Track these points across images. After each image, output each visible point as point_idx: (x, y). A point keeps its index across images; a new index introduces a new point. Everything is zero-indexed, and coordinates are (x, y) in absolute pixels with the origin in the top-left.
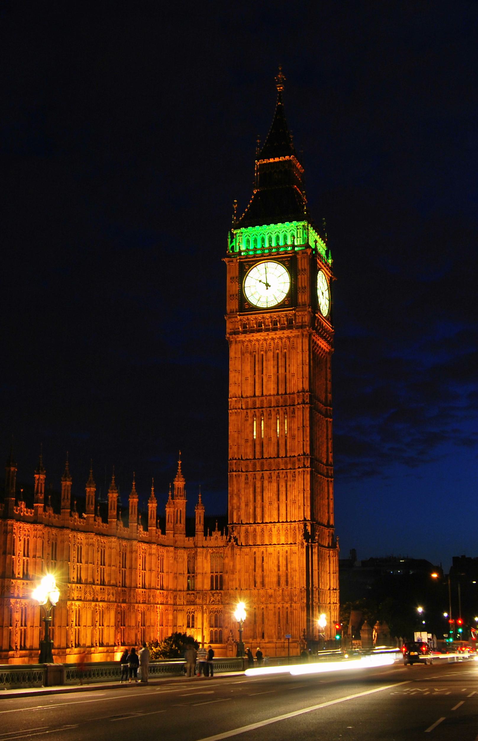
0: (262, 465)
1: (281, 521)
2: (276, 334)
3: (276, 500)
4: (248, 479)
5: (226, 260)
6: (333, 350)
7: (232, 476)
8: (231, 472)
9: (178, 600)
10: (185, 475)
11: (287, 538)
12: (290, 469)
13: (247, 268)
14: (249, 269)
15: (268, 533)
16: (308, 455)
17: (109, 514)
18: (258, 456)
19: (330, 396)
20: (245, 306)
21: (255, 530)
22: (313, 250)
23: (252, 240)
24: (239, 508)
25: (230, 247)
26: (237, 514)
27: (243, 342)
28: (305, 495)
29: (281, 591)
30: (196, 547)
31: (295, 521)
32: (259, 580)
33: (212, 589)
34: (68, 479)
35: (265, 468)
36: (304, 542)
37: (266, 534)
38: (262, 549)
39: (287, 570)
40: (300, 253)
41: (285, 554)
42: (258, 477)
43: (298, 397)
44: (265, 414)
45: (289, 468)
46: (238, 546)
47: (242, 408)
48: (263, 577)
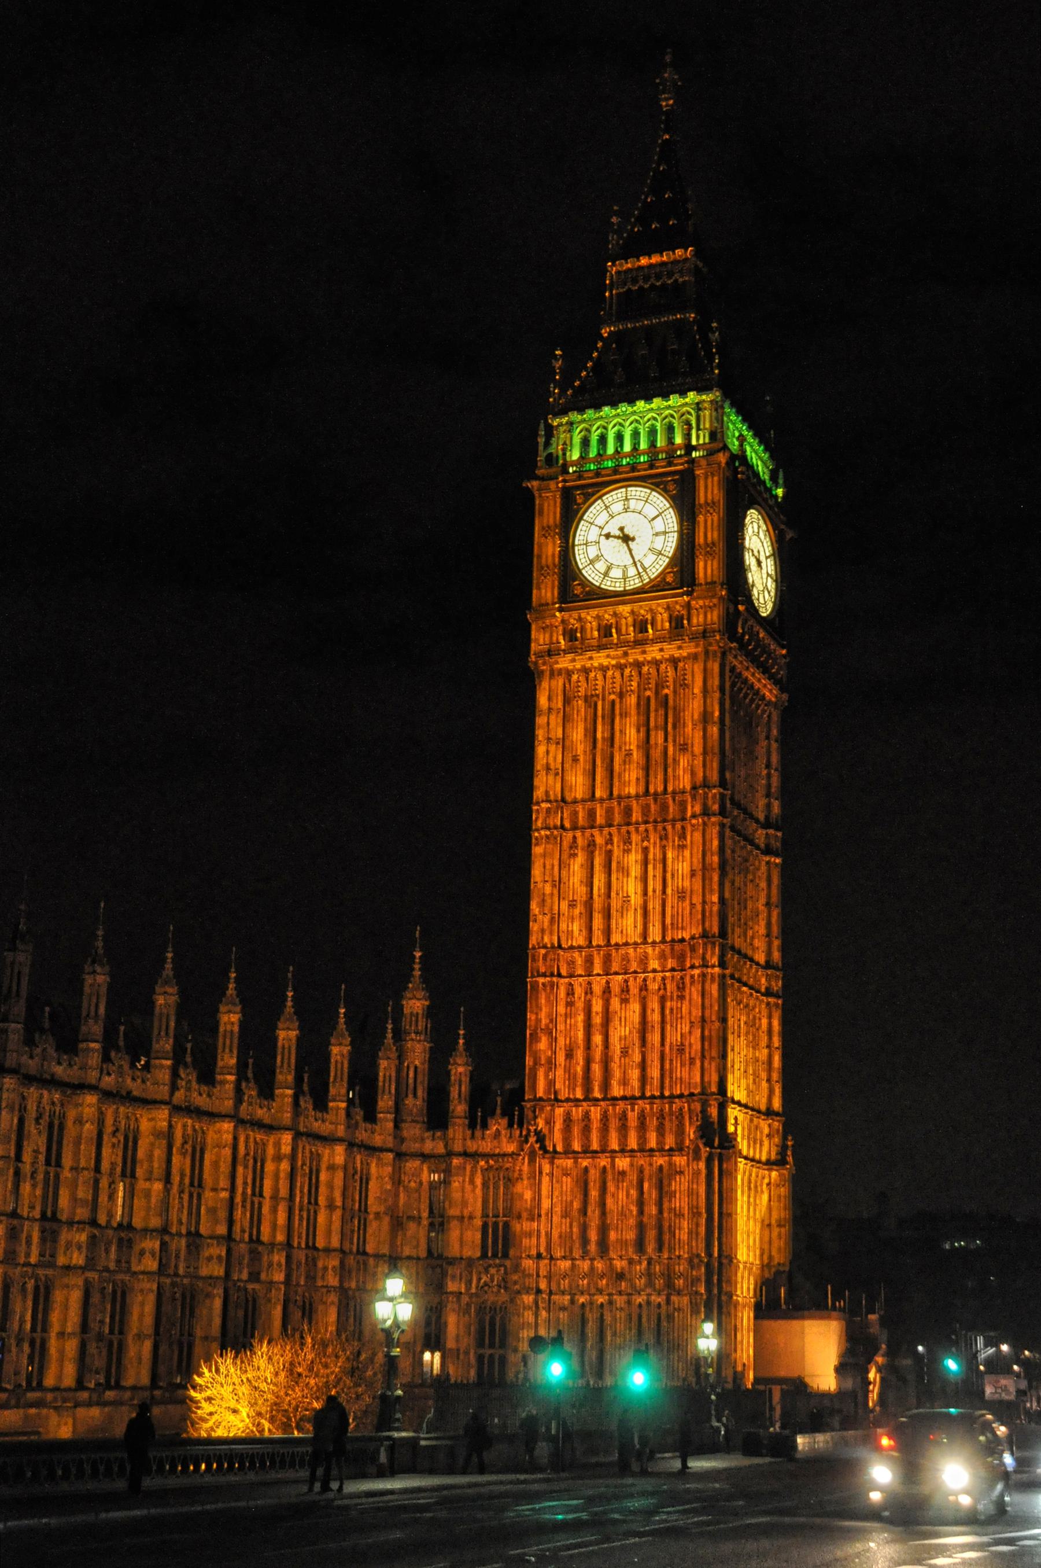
0: (607, 960)
1: (648, 1094)
4: (573, 994)
5: (535, 484)
6: (785, 696)
7: (535, 986)
8: (533, 976)
13: (579, 501)
14: (584, 503)
16: (714, 936)
17: (220, 1064)
18: (598, 939)
19: (776, 807)
20: (573, 588)
21: (587, 1116)
22: (733, 457)
23: (594, 438)
24: (551, 1064)
25: (541, 457)
26: (546, 1076)
27: (569, 673)
28: (707, 1033)
31: (681, 1096)
32: (593, 1236)
34: (99, 969)
35: (615, 967)
36: (701, 1146)
39: (661, 1211)
40: (703, 462)
42: (597, 989)
43: (694, 798)
44: (615, 840)
45: (669, 966)
46: (546, 1151)
47: (562, 827)
48: (604, 1230)
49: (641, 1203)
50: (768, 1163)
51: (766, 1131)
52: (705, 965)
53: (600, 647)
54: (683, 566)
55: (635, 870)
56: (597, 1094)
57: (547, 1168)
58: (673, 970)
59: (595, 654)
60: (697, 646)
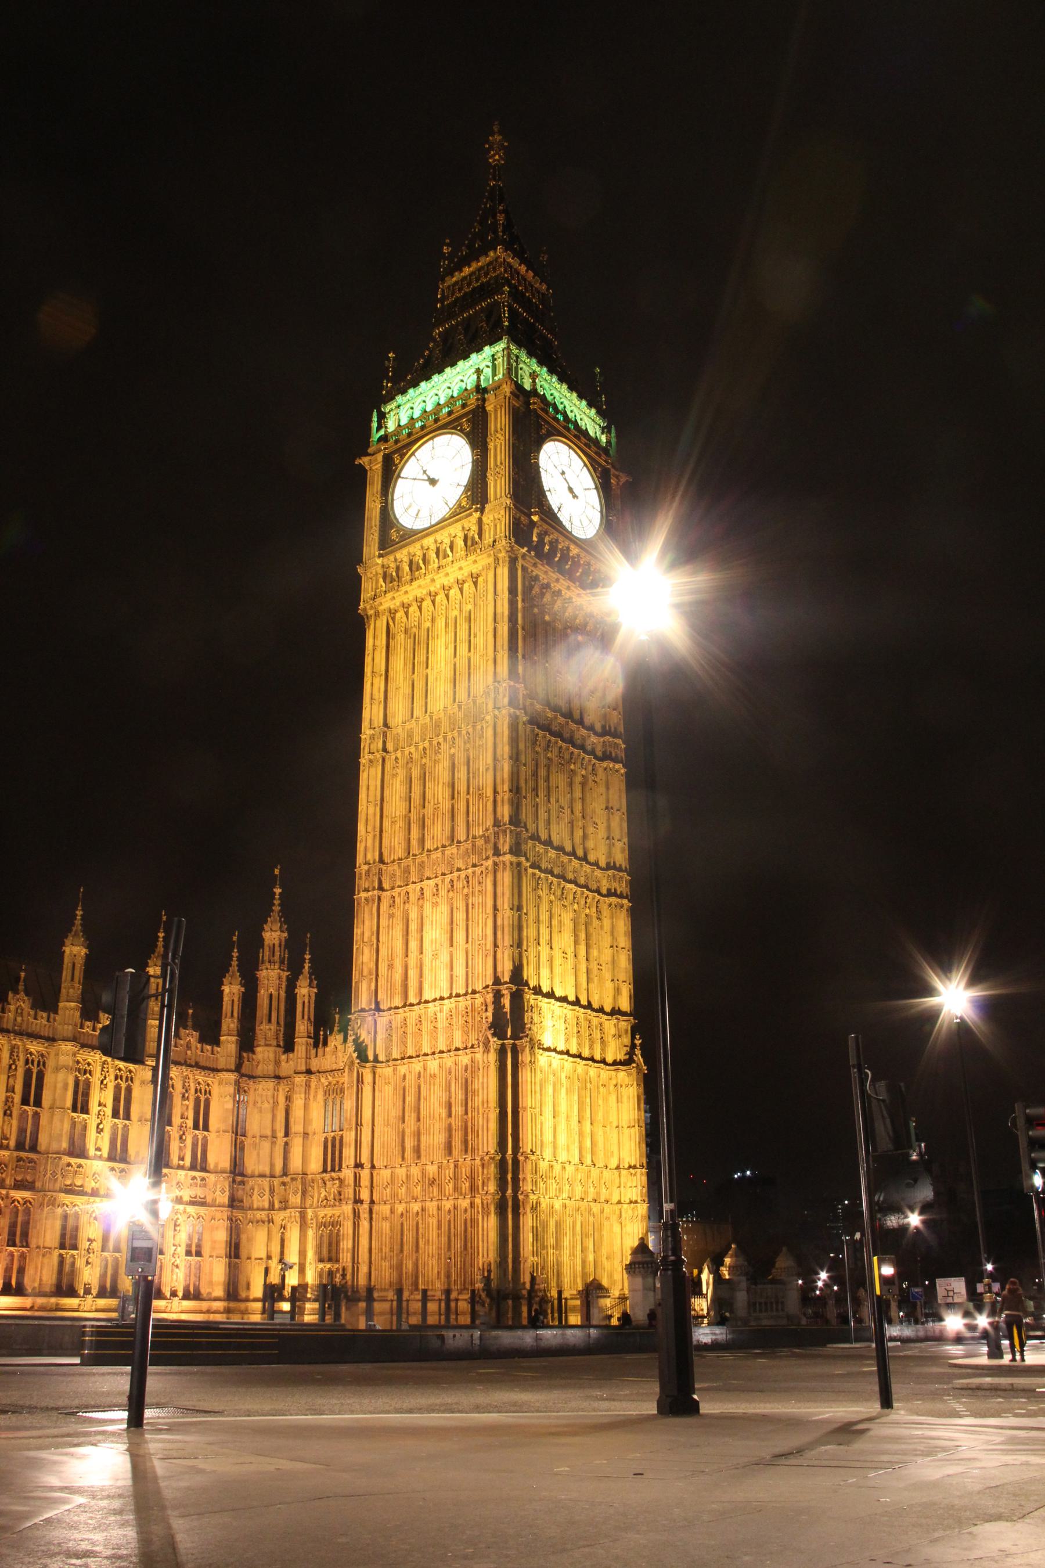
3: (446, 943)
9: (255, 1197)
10: (289, 919)
11: (467, 1033)
12: (474, 866)
15: (431, 1027)
18: (415, 848)
25: (376, 436)
27: (392, 613)
28: (499, 922)
29: (452, 1166)
32: (409, 1144)
33: (325, 1171)
36: (490, 1037)
37: (426, 1027)
38: (417, 1066)
39: (466, 1113)
41: (461, 1073)
47: (385, 750)
48: (418, 1134)
49: (449, 1106)
50: (615, 1063)
51: (613, 1031)
54: (477, 491)
56: (412, 999)
59: (407, 588)
60: (489, 556)
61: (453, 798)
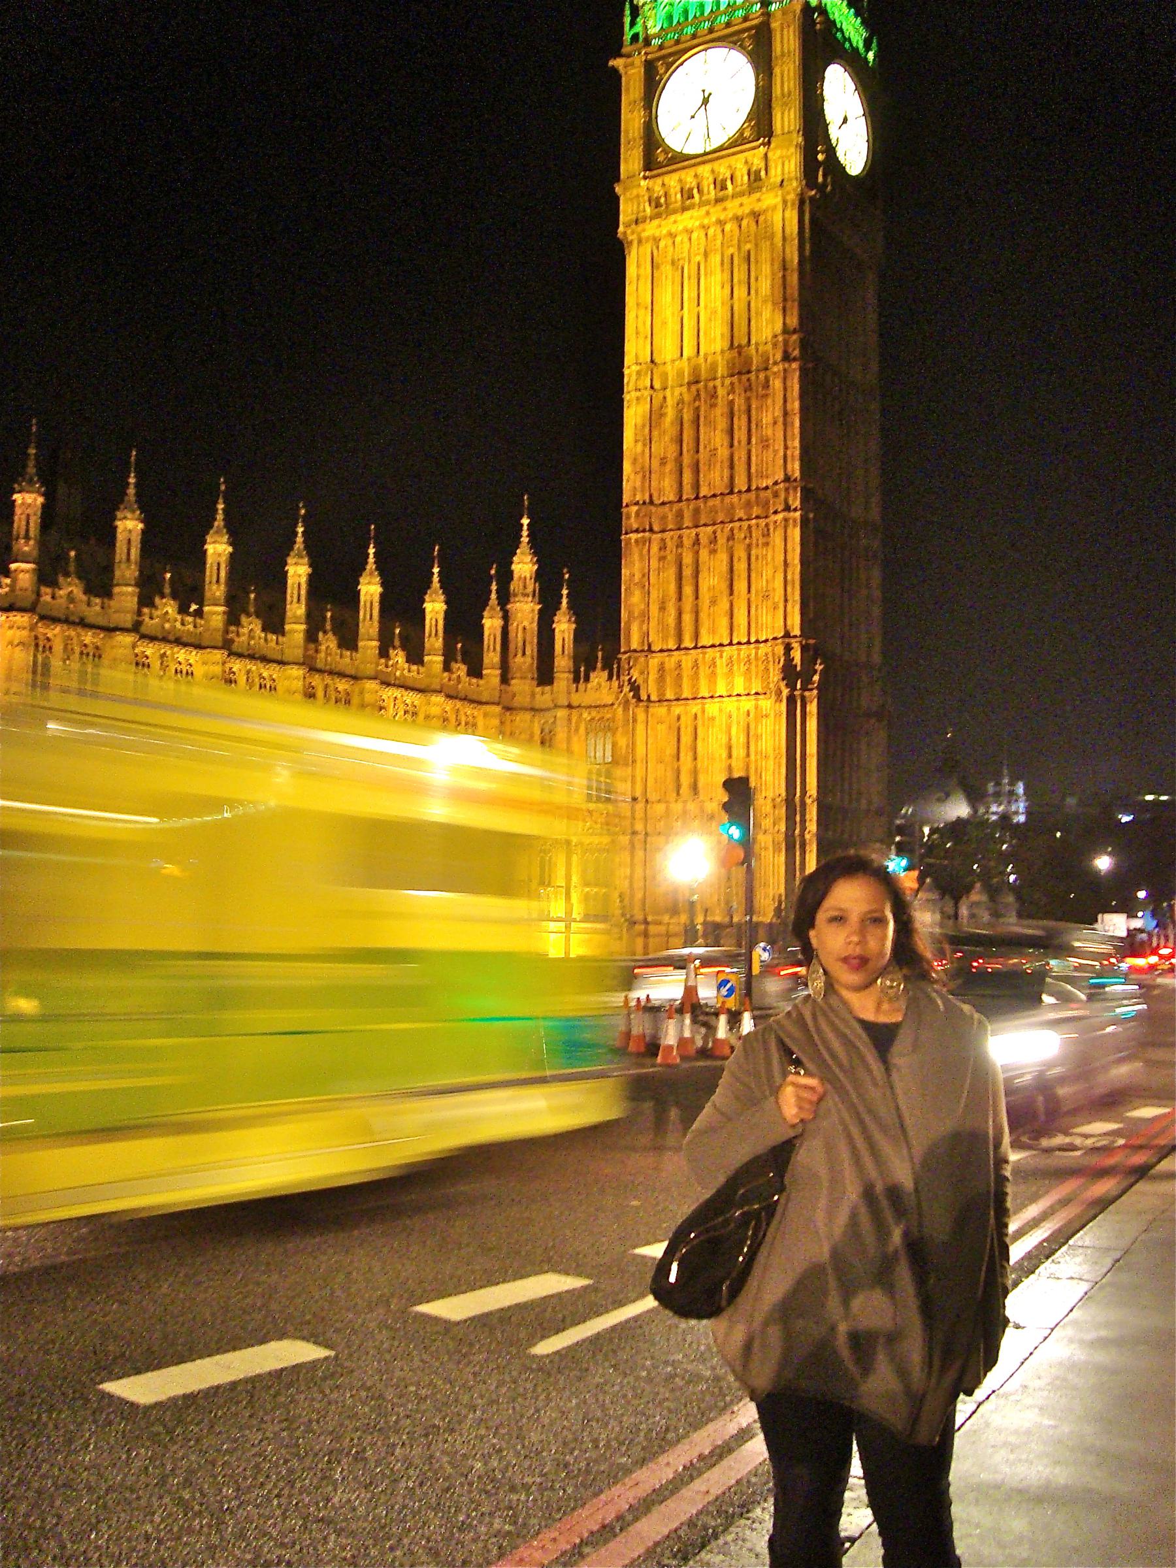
1: (735, 642)
2: (725, 209)
3: (726, 592)
12: (757, 517)
18: (688, 492)
21: (679, 665)
24: (645, 616)
25: (628, 36)
26: (641, 628)
27: (656, 240)
30: (556, 706)
32: (685, 780)
34: (129, 515)
37: (704, 672)
39: (748, 755)
46: (639, 700)
48: (695, 772)
52: (787, 508)
53: (684, 209)
55: (722, 424)
56: (688, 643)
57: (641, 716)
58: (757, 517)
59: (678, 217)
61: (732, 446)
